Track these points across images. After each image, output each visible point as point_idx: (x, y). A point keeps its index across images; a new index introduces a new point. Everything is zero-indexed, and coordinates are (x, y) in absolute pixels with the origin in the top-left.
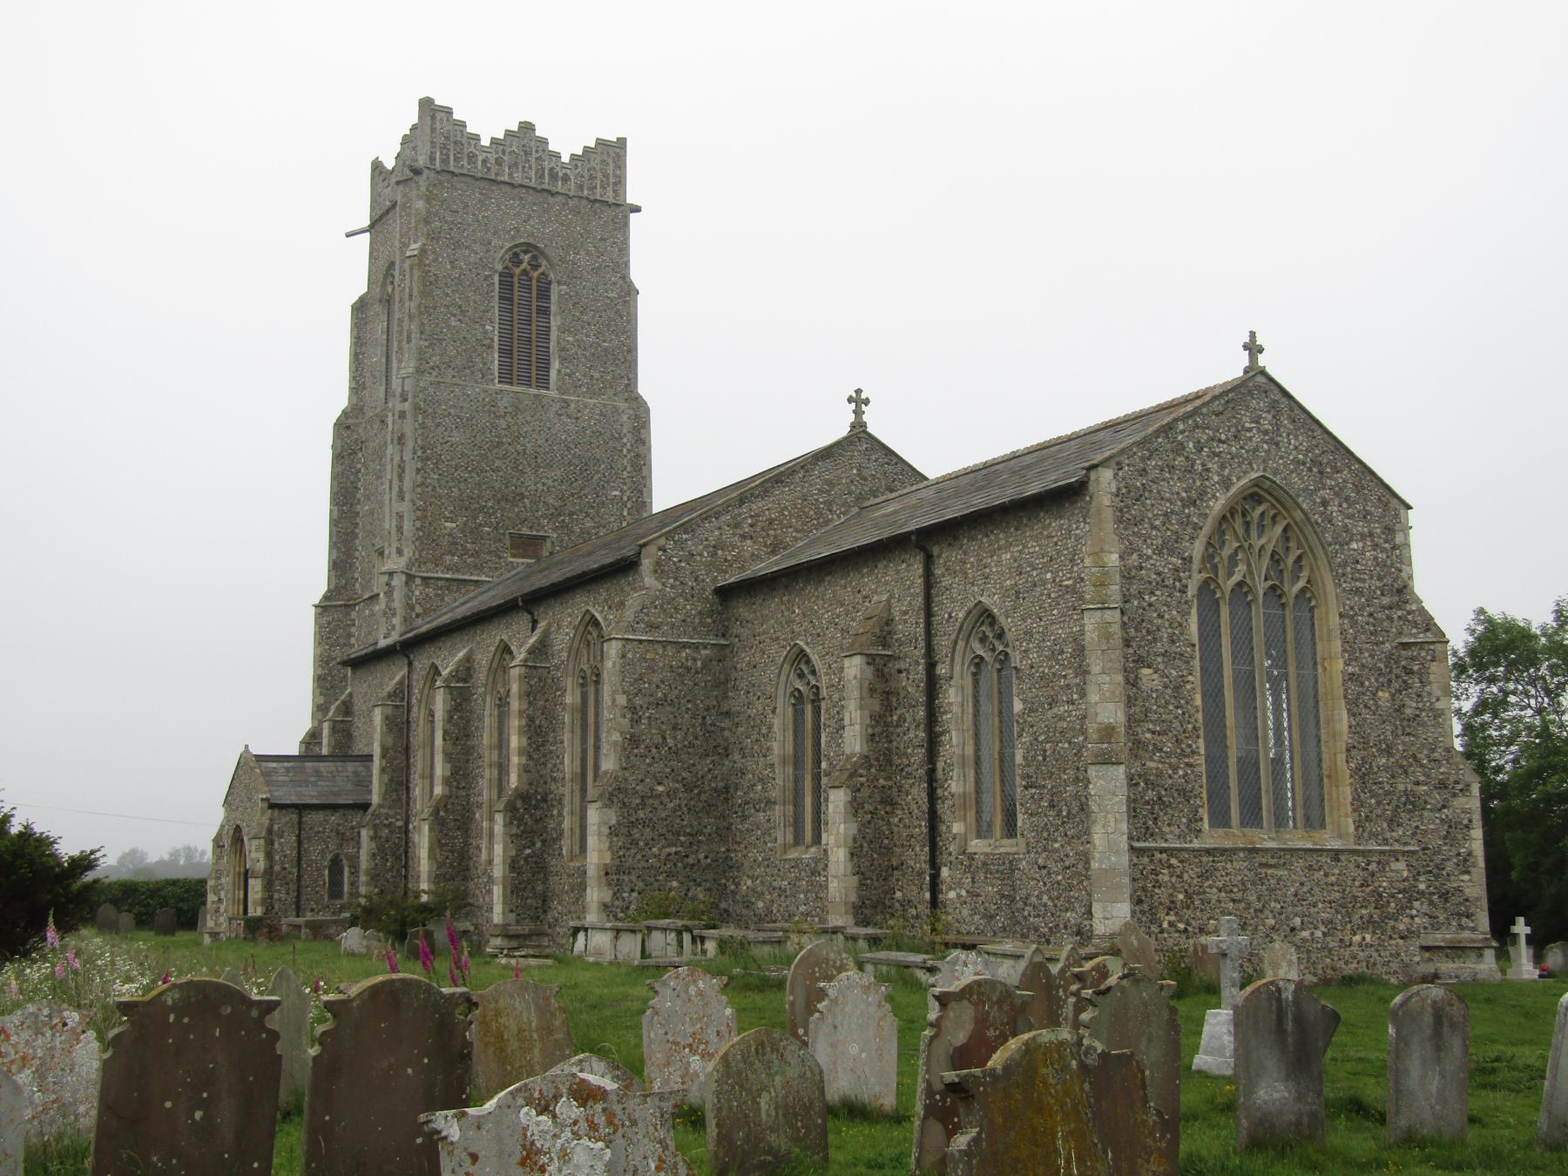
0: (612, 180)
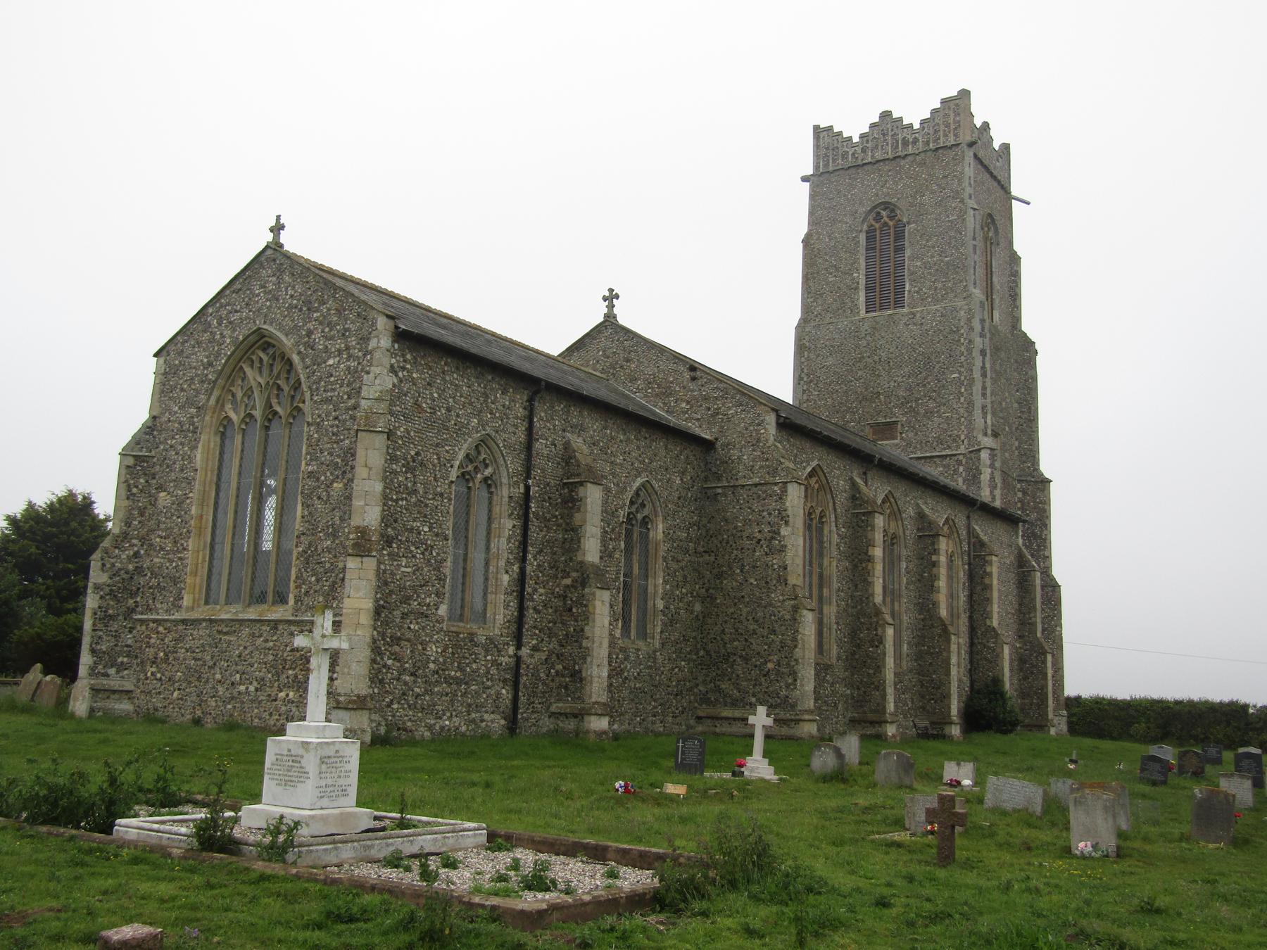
0: (953, 127)
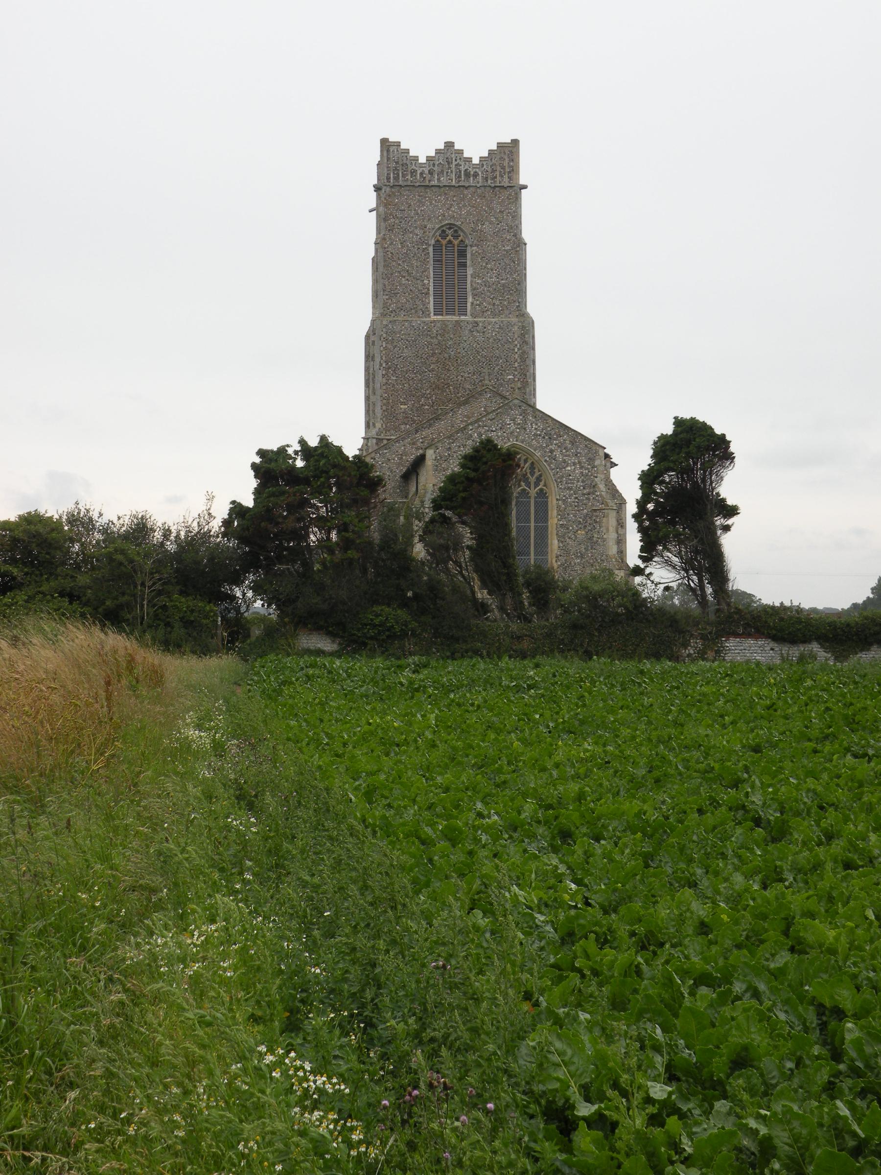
0: (507, 170)
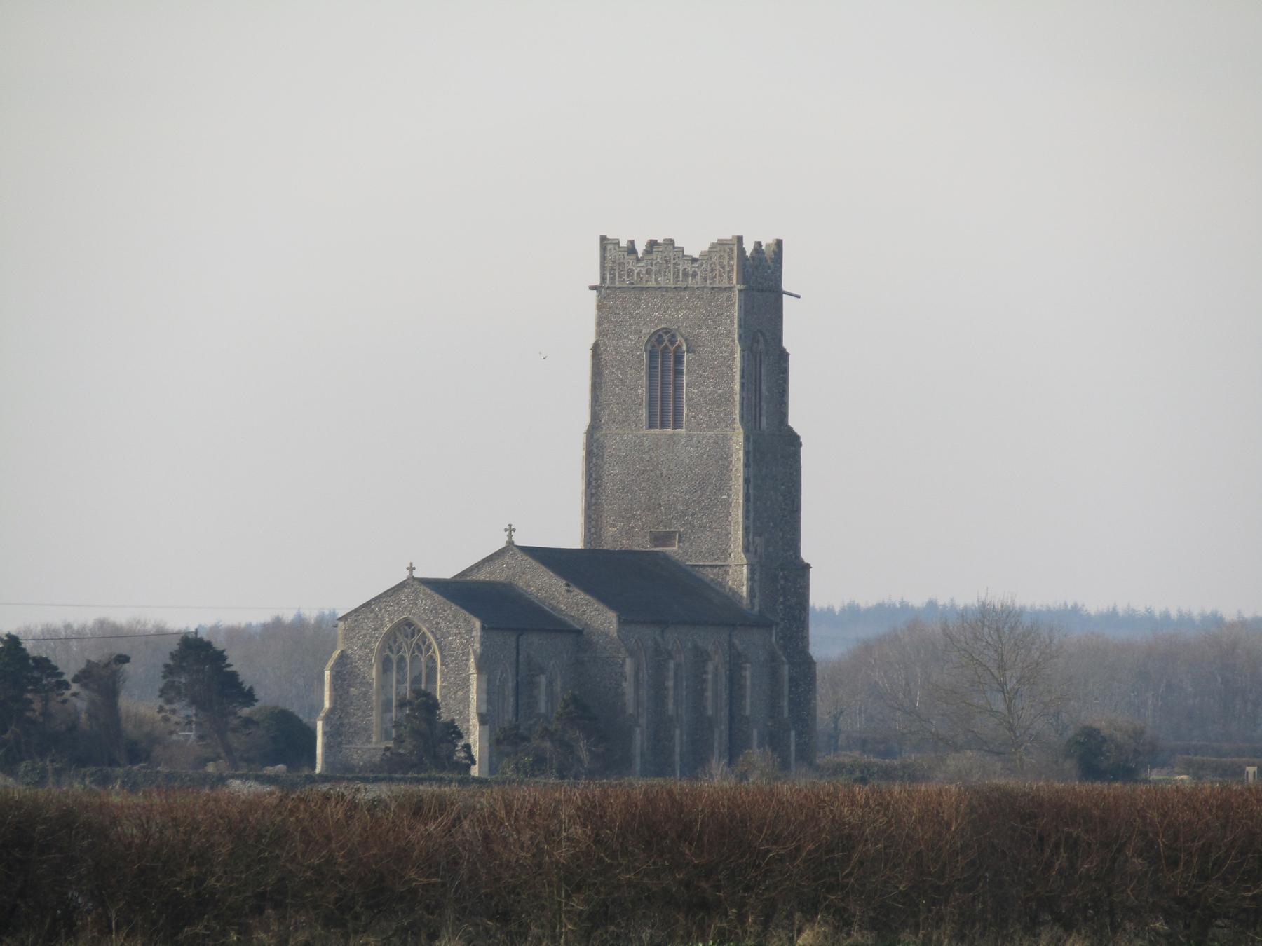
0: (727, 269)
